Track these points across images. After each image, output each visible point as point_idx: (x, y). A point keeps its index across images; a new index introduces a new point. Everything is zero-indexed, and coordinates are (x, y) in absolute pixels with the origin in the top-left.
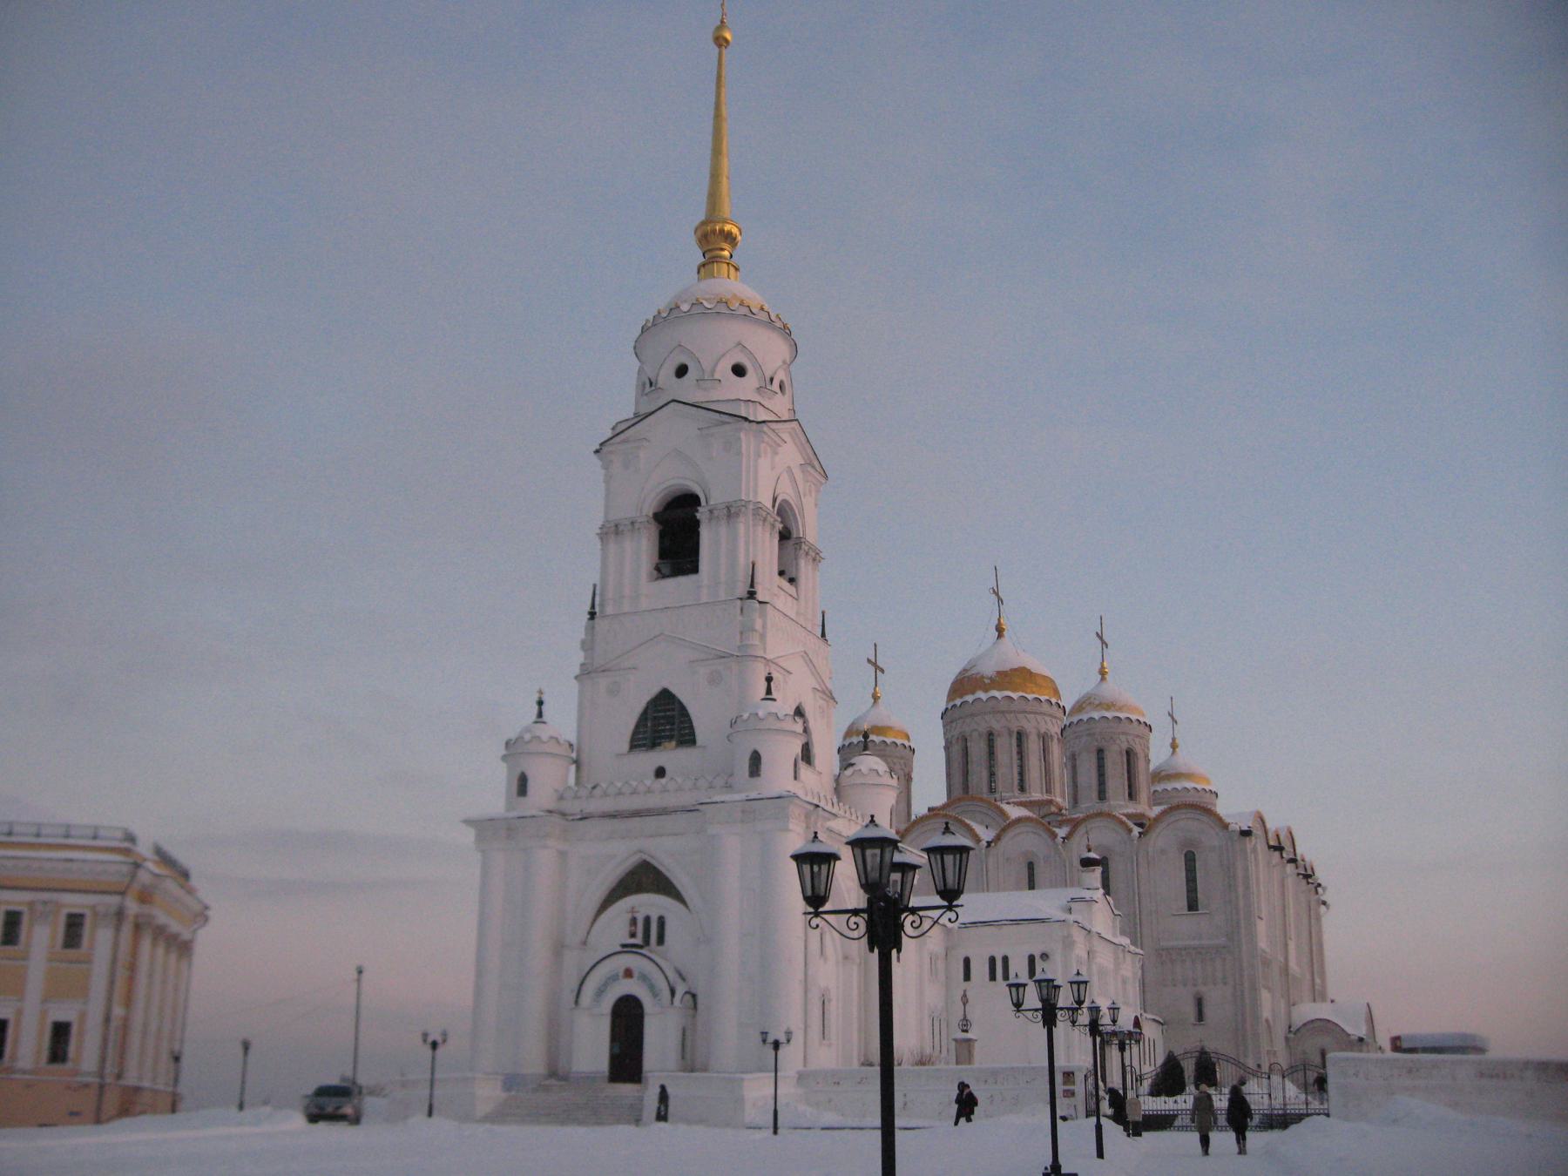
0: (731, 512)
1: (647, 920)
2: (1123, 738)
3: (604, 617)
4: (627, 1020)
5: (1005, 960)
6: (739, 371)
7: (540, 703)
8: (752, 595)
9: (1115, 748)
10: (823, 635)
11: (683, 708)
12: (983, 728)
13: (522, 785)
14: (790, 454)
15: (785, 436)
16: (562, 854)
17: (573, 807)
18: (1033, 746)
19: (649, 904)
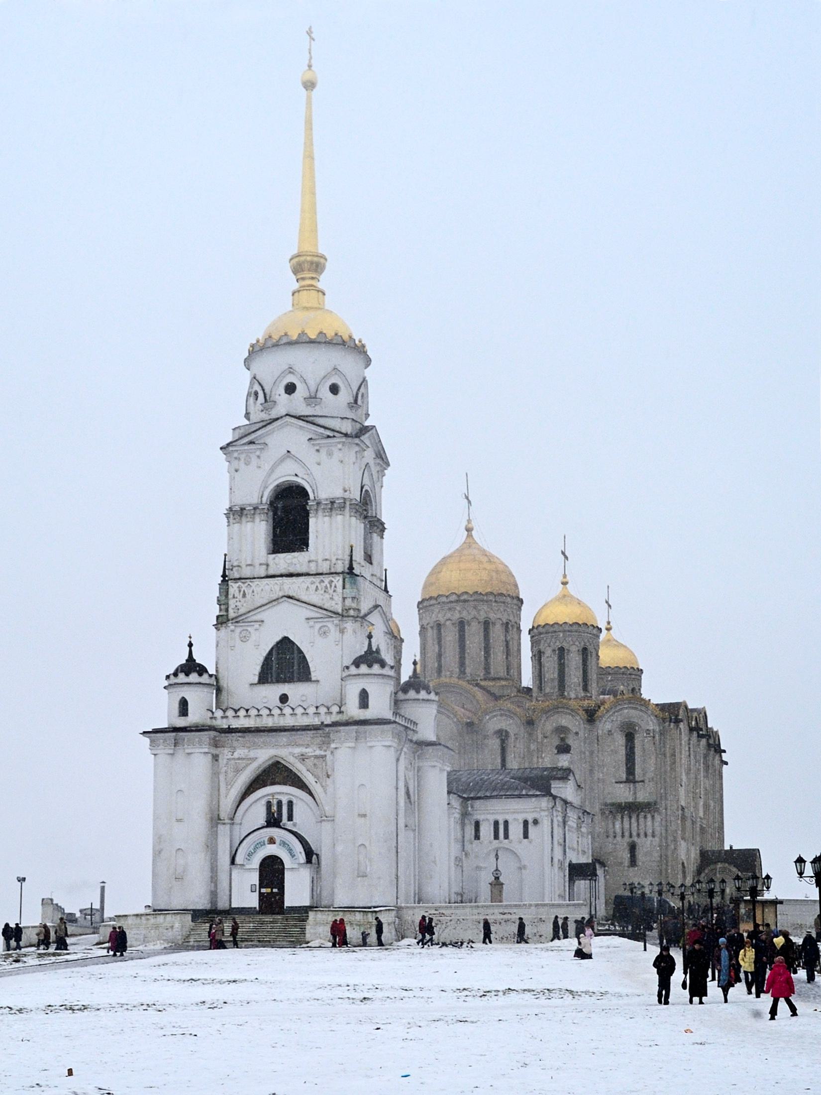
0: (333, 506)
1: (280, 803)
3: (236, 580)
4: (272, 872)
5: (506, 823)
6: (334, 389)
7: (190, 645)
8: (351, 568)
9: (574, 649)
10: (386, 590)
11: (300, 651)
12: (457, 616)
14: (369, 455)
15: (368, 443)
16: (215, 758)
18: (497, 632)
19: (282, 792)
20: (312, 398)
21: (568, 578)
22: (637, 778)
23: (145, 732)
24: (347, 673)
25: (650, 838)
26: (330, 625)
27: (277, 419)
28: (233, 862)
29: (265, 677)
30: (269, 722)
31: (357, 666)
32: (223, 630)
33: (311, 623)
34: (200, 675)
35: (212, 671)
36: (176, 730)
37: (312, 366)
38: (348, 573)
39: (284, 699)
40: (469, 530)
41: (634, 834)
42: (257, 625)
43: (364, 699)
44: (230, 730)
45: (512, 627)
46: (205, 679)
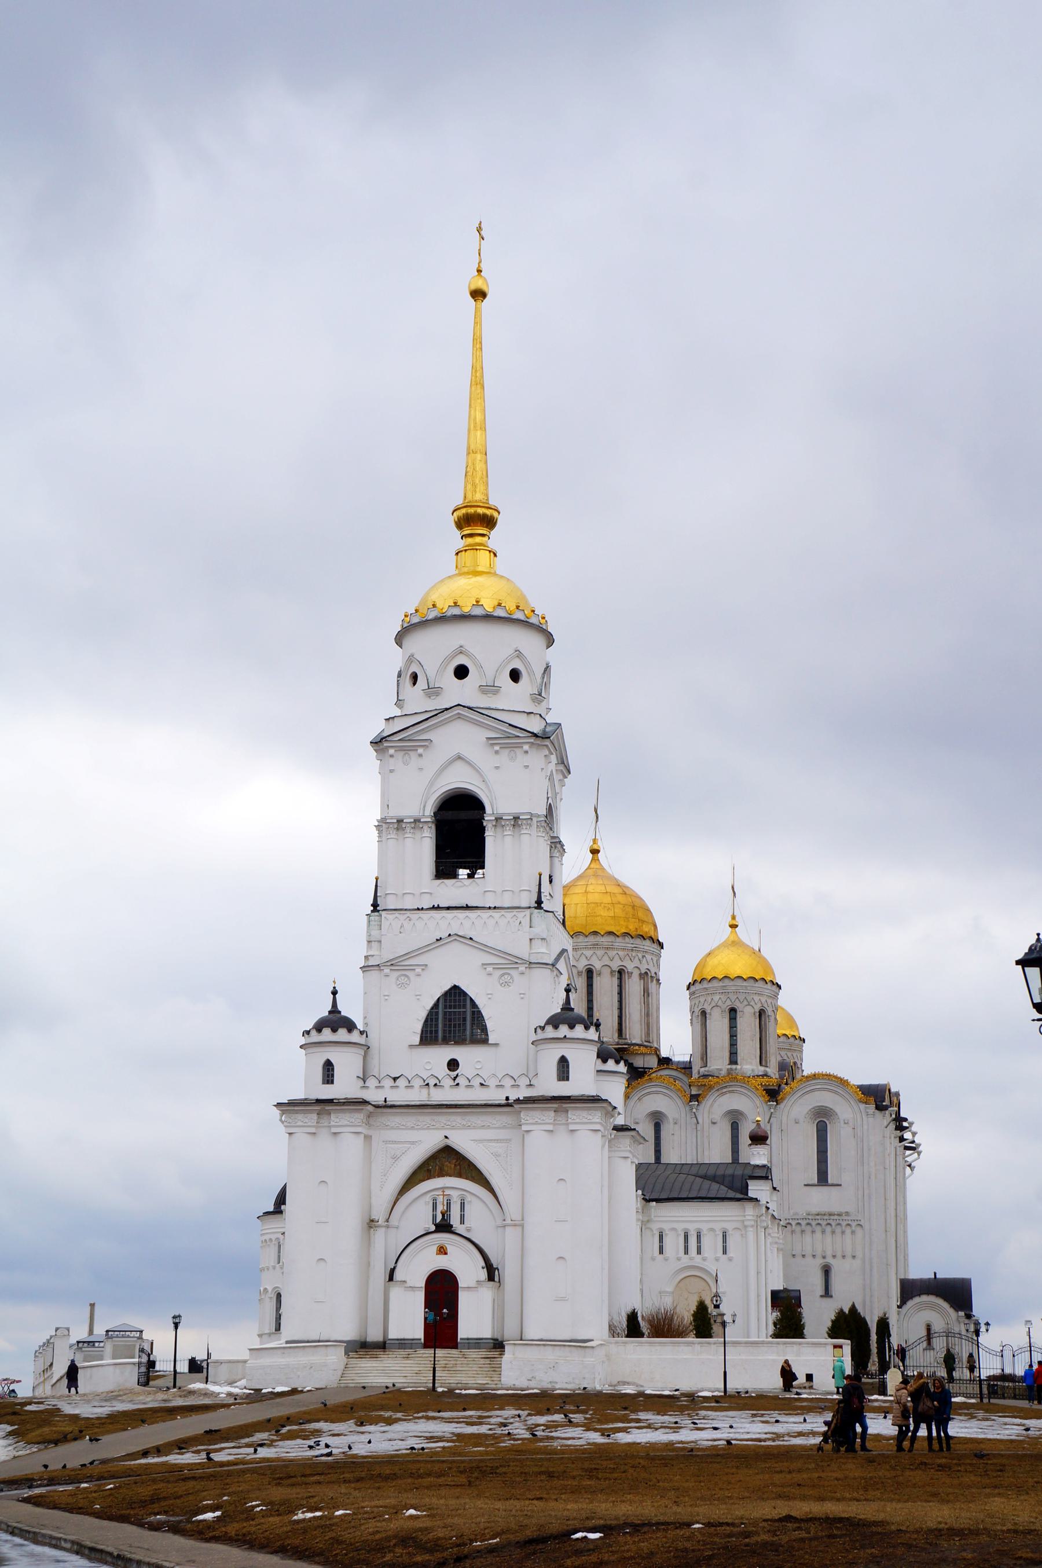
2: (757, 998)
4: (442, 1290)
5: (699, 1237)
6: (515, 676)
7: (334, 993)
8: (539, 903)
9: (748, 1010)
13: (328, 1072)
16: (368, 1138)
17: (375, 1096)
18: (634, 987)
20: (490, 689)
21: (739, 921)
22: (830, 1181)
23: (279, 1105)
24: (541, 1035)
25: (849, 1259)
26: (513, 972)
27: (447, 709)
28: (391, 1278)
29: (429, 1036)
30: (438, 1096)
31: (556, 1027)
32: (374, 974)
33: (490, 969)
34: (350, 1031)
35: (360, 1026)
36: (319, 1101)
37: (490, 649)
38: (536, 908)
39: (453, 1065)
40: (595, 852)
41: (829, 1253)
42: (418, 970)
43: (563, 1068)
44: (387, 1106)
45: (650, 978)
46: (355, 1037)
